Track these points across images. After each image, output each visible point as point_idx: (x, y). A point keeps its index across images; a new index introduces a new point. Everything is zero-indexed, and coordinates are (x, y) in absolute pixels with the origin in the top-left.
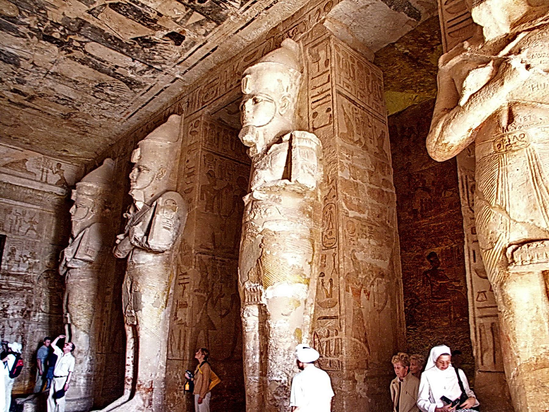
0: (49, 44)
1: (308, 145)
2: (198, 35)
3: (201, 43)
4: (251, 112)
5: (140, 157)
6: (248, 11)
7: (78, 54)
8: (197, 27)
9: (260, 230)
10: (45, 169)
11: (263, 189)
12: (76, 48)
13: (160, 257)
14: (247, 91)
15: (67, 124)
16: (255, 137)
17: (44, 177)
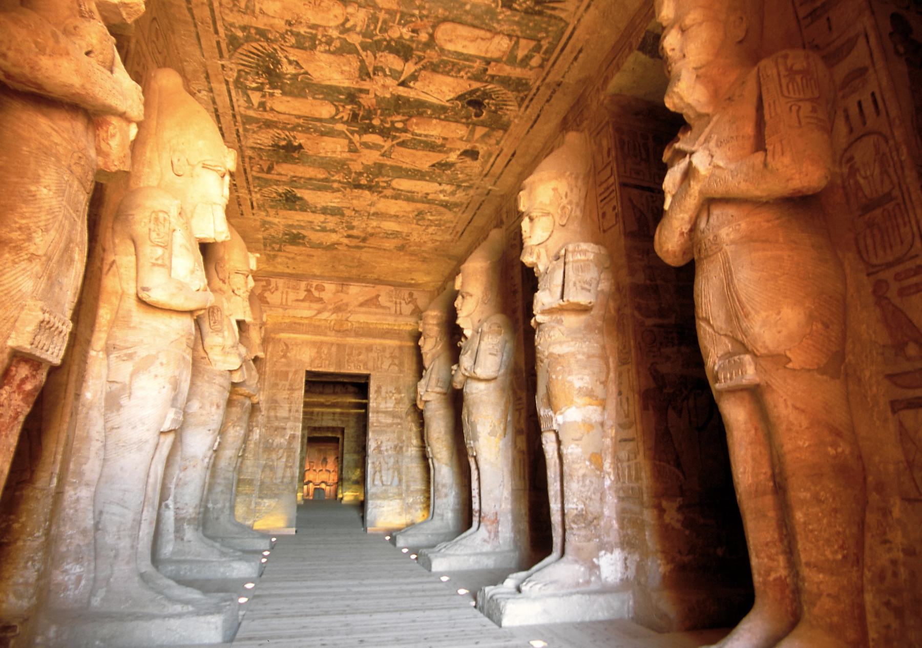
0: (360, 191)
1: (583, 257)
2: (490, 145)
3: (498, 152)
4: (528, 230)
5: (463, 283)
6: (529, 110)
7: (388, 192)
8: (487, 140)
9: (546, 354)
10: (398, 301)
11: (543, 312)
12: (384, 188)
13: (492, 384)
14: (522, 208)
15: (404, 255)
16: (535, 256)
17: (398, 309)
